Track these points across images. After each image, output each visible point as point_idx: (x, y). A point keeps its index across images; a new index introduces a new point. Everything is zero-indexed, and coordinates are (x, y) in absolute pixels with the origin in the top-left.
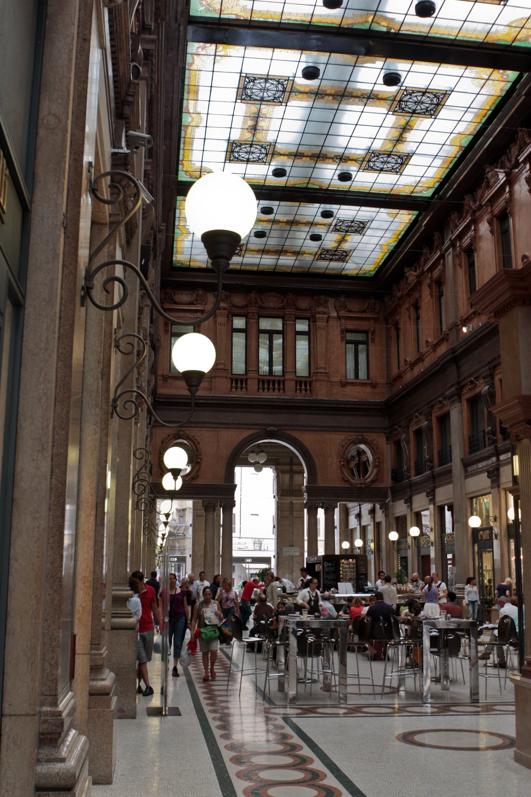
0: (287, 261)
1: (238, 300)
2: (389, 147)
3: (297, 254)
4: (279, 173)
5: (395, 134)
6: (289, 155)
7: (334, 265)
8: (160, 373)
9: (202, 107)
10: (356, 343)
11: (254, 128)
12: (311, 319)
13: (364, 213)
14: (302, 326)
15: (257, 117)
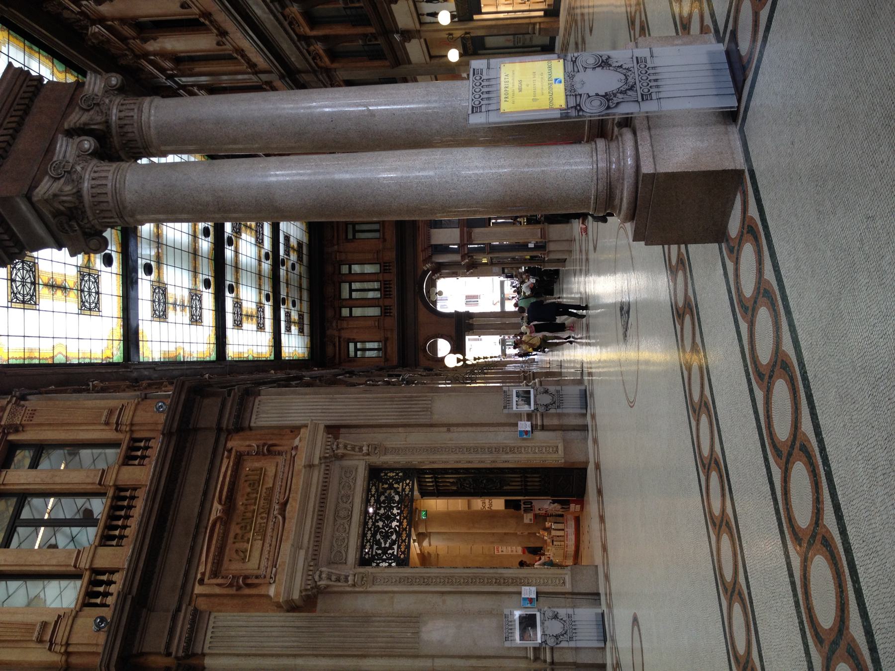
0: (305, 284)
1: (330, 313)
2: (253, 233)
3: (301, 276)
4: (268, 299)
5: (248, 231)
6: (260, 293)
7: (305, 251)
8: (382, 364)
9: (246, 348)
10: (355, 232)
11: (252, 316)
12: (341, 263)
13: (282, 240)
14: (345, 269)
15: (247, 316)
